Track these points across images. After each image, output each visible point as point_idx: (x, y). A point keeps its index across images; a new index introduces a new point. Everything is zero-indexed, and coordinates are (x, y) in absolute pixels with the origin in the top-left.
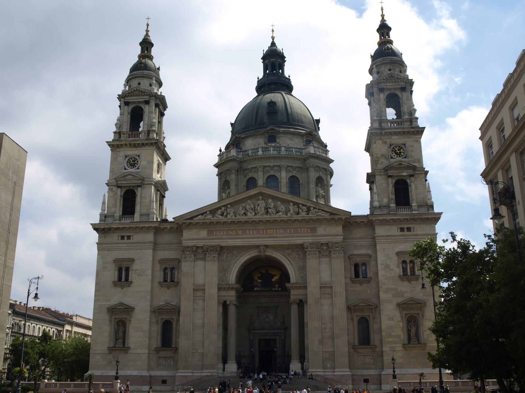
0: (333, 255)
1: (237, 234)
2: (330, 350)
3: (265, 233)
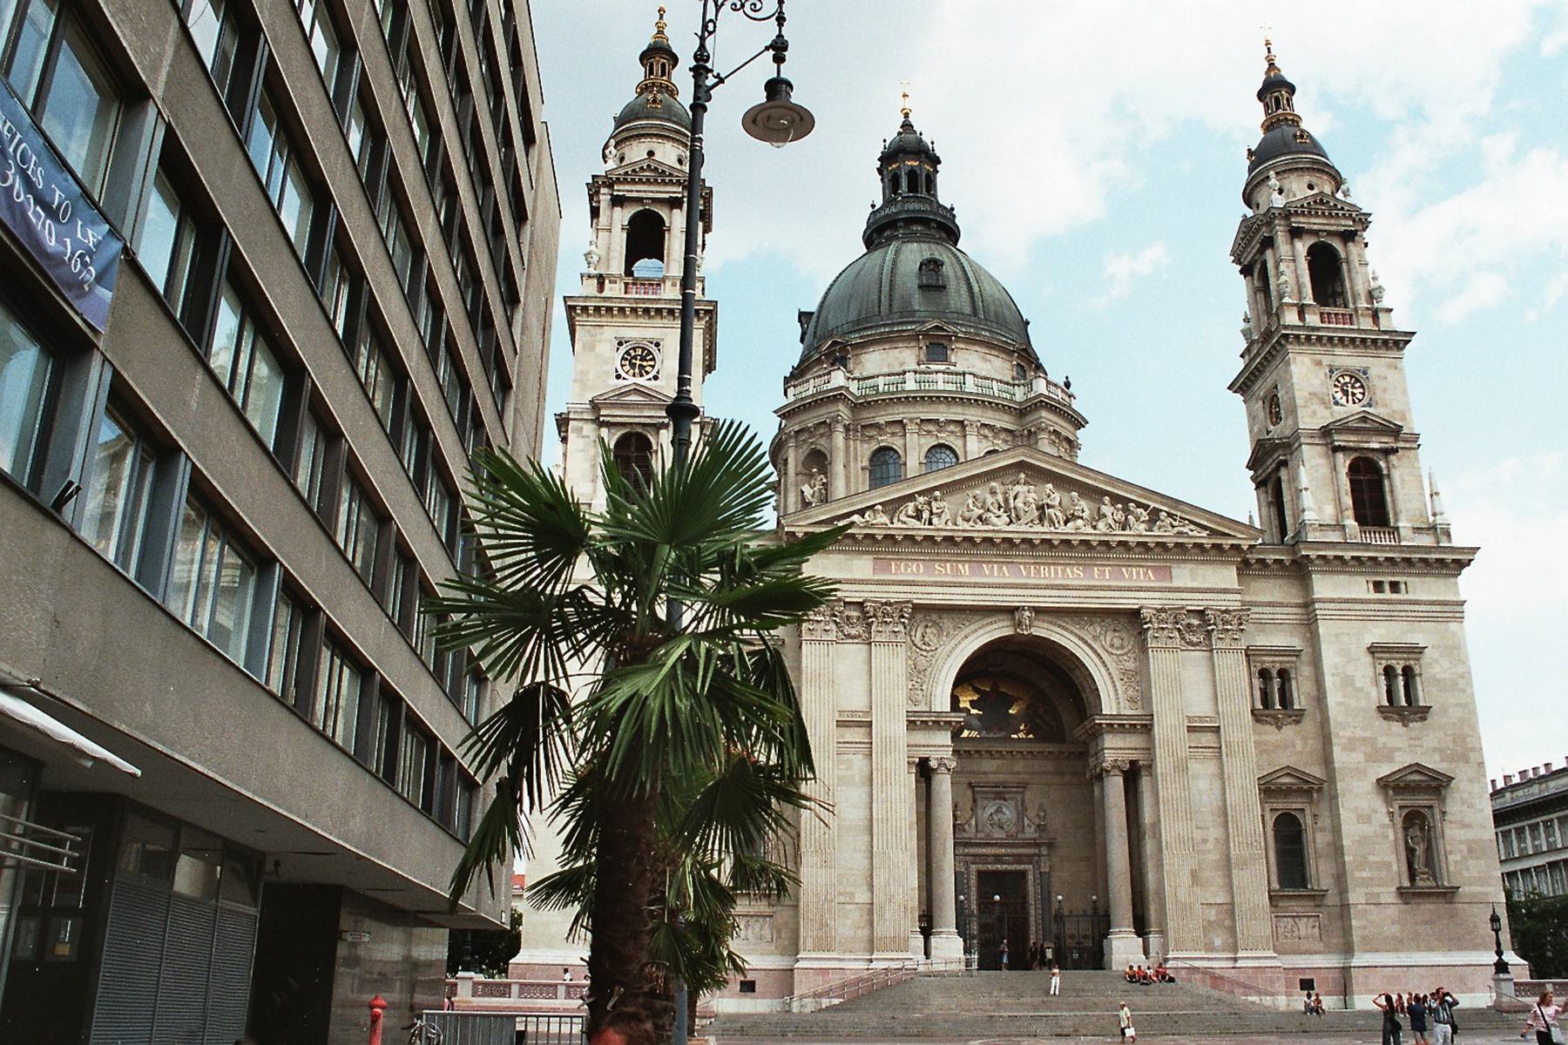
0: (1216, 644)
1: (958, 573)
2: (1219, 901)
3: (1033, 575)
